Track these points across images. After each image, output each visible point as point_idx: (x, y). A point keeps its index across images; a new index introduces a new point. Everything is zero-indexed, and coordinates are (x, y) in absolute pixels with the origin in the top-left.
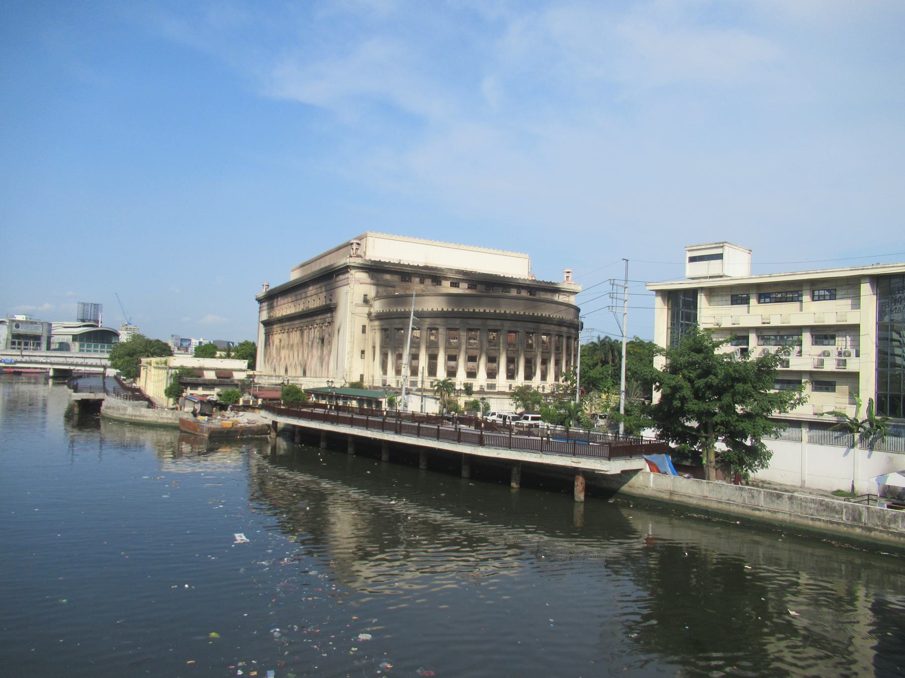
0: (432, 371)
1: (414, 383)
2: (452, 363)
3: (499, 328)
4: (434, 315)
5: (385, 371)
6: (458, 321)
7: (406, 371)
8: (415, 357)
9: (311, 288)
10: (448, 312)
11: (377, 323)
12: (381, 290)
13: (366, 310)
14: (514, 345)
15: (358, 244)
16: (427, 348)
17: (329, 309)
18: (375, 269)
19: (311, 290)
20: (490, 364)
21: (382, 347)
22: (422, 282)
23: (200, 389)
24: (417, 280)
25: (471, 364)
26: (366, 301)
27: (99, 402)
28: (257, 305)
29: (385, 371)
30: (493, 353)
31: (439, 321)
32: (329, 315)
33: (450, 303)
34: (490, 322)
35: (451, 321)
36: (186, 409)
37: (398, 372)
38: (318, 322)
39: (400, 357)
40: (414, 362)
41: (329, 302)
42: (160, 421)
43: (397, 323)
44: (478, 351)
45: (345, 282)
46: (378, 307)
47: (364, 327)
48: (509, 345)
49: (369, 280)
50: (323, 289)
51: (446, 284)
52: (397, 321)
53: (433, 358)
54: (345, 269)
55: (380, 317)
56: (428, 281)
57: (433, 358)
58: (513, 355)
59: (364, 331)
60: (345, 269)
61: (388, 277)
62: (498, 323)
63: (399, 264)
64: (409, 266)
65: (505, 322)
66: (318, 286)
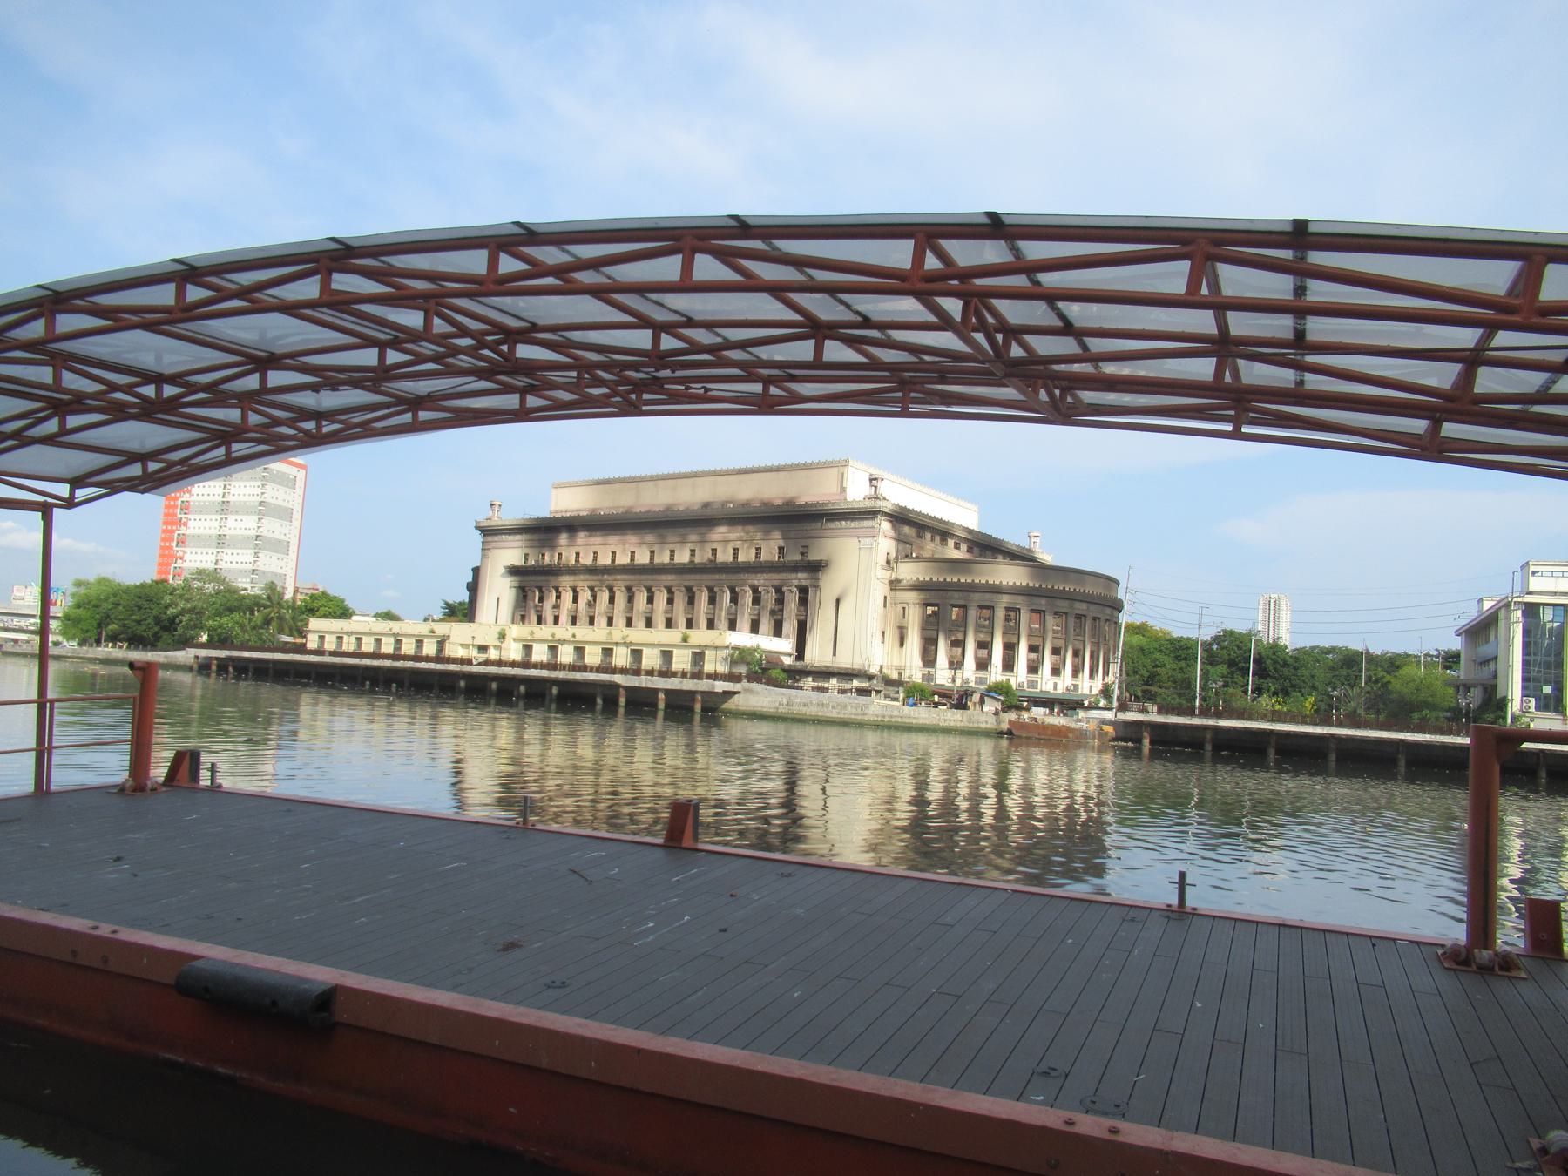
0: (1009, 665)
2: (1034, 656)
4: (1015, 591)
5: (929, 659)
6: (1043, 601)
8: (984, 645)
9: (722, 529)
10: (1034, 588)
11: (913, 594)
12: (901, 546)
13: (887, 575)
16: (1004, 634)
17: (816, 568)
18: (900, 517)
19: (721, 532)
21: (923, 629)
22: (932, 539)
23: (834, 681)
24: (929, 536)
25: (1055, 657)
26: (888, 562)
27: (728, 694)
28: (478, 537)
29: (929, 659)
31: (1020, 599)
32: (800, 575)
33: (1033, 577)
34: (1077, 605)
35: (1036, 600)
36: (986, 709)
37: (956, 664)
38: (756, 583)
39: (959, 644)
40: (983, 653)
41: (798, 557)
42: (942, 723)
43: (957, 598)
45: (838, 532)
46: (909, 572)
49: (891, 533)
50: (777, 535)
51: (951, 543)
52: (956, 595)
53: (1010, 647)
54: (872, 514)
55: (919, 587)
56: (938, 538)
57: (1010, 647)
60: (872, 514)
61: (906, 529)
63: (919, 514)
64: (927, 516)
66: (751, 528)
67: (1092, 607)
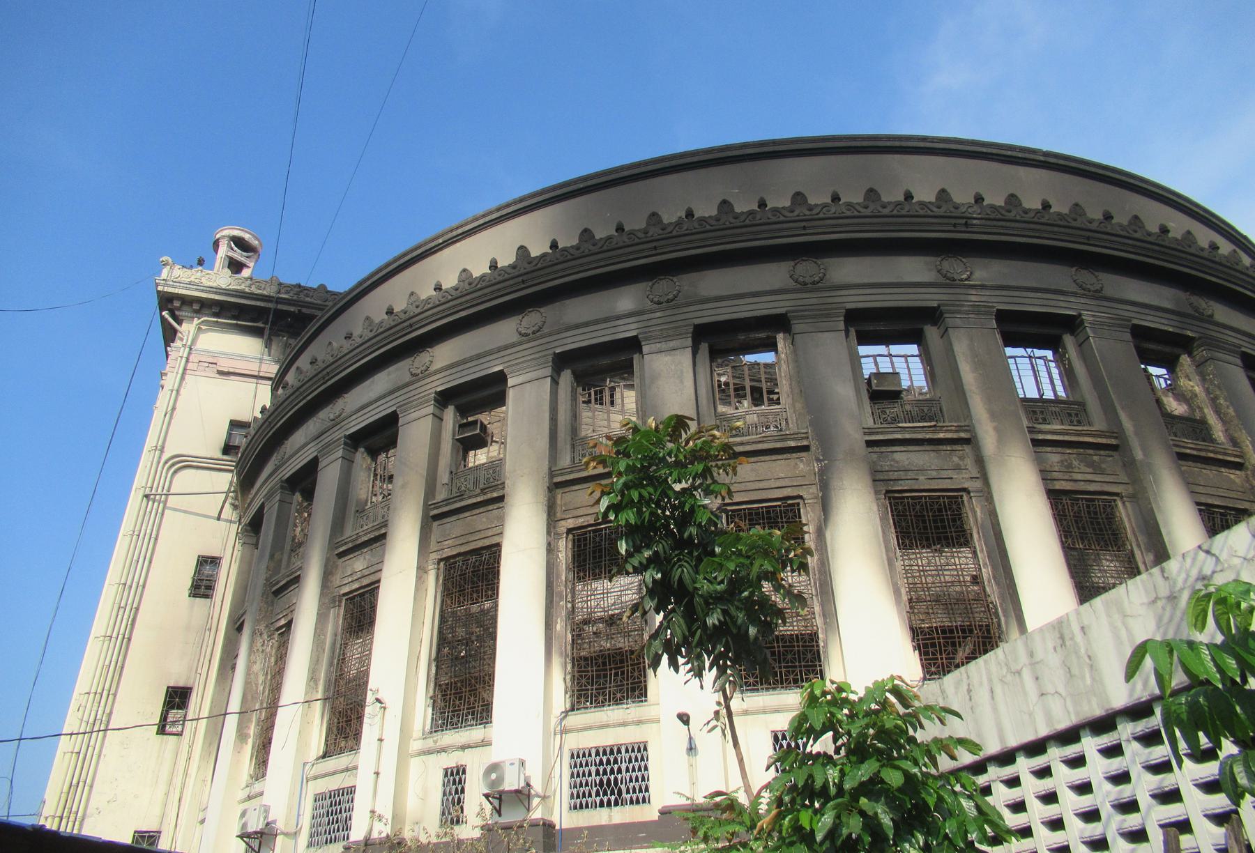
0: (463, 686)
1: (334, 810)
3: (930, 299)
6: (625, 300)
7: (300, 723)
8: (359, 613)
14: (1071, 409)
15: (240, 243)
16: (433, 517)
20: (924, 558)
30: (924, 470)
34: (848, 270)
44: (803, 466)
47: (208, 563)
48: (1037, 408)
58: (1084, 477)
59: (202, 587)
62: (914, 269)
65: (956, 267)
67: (985, 271)
